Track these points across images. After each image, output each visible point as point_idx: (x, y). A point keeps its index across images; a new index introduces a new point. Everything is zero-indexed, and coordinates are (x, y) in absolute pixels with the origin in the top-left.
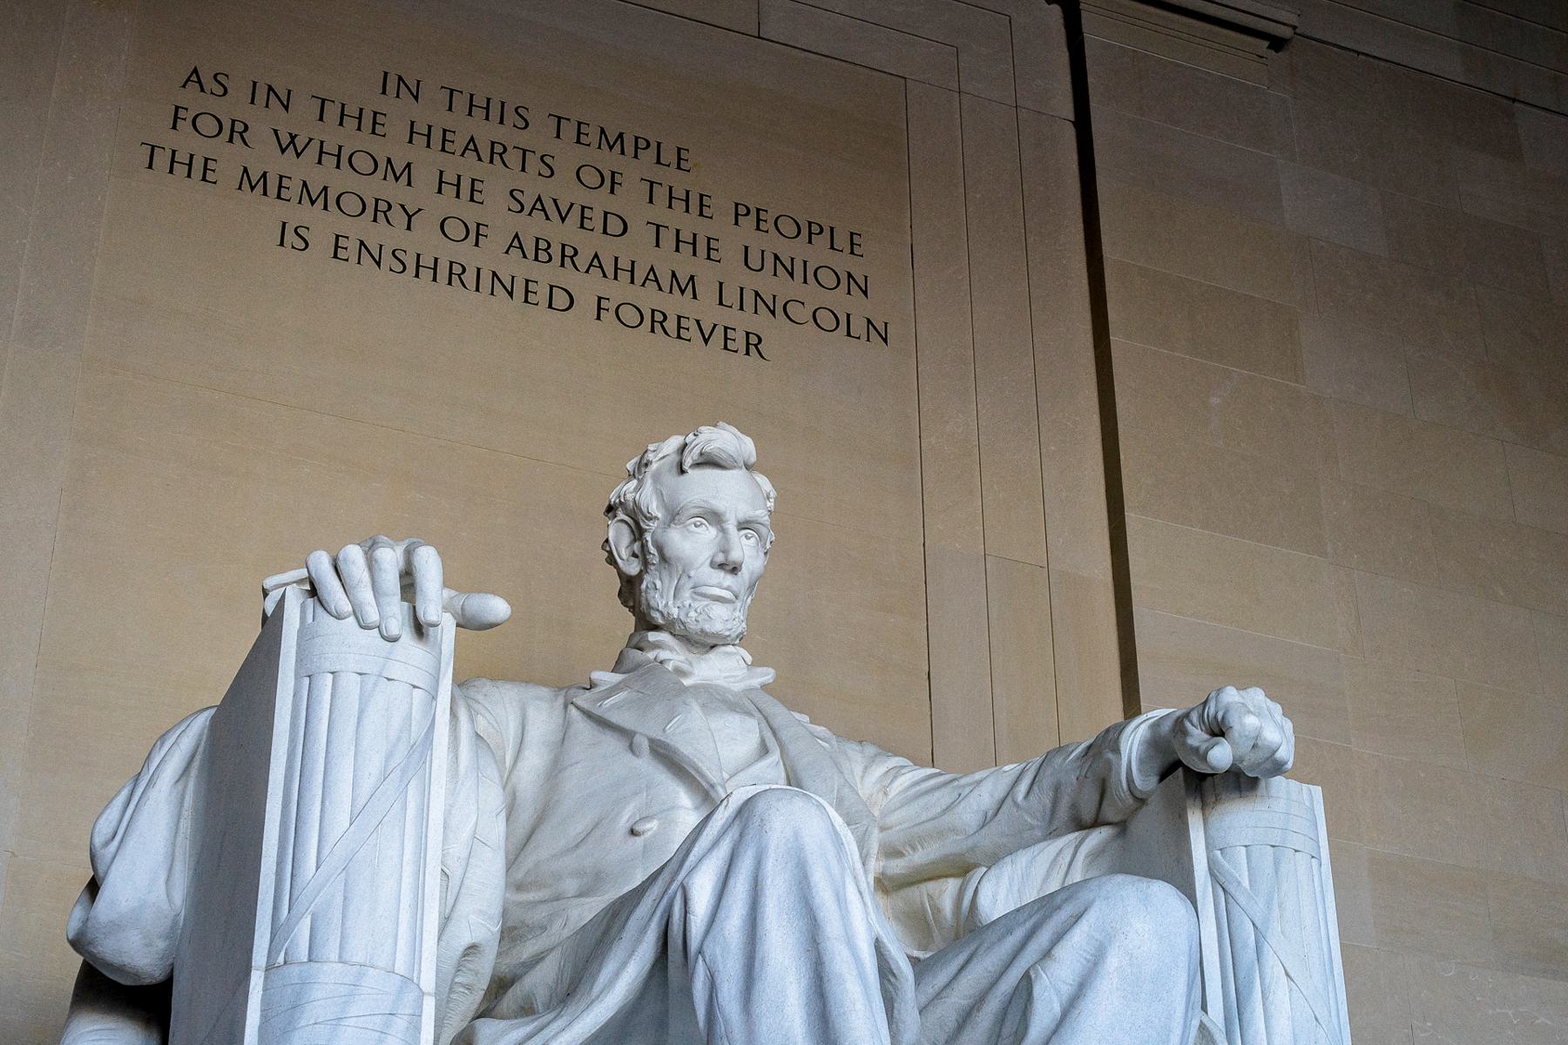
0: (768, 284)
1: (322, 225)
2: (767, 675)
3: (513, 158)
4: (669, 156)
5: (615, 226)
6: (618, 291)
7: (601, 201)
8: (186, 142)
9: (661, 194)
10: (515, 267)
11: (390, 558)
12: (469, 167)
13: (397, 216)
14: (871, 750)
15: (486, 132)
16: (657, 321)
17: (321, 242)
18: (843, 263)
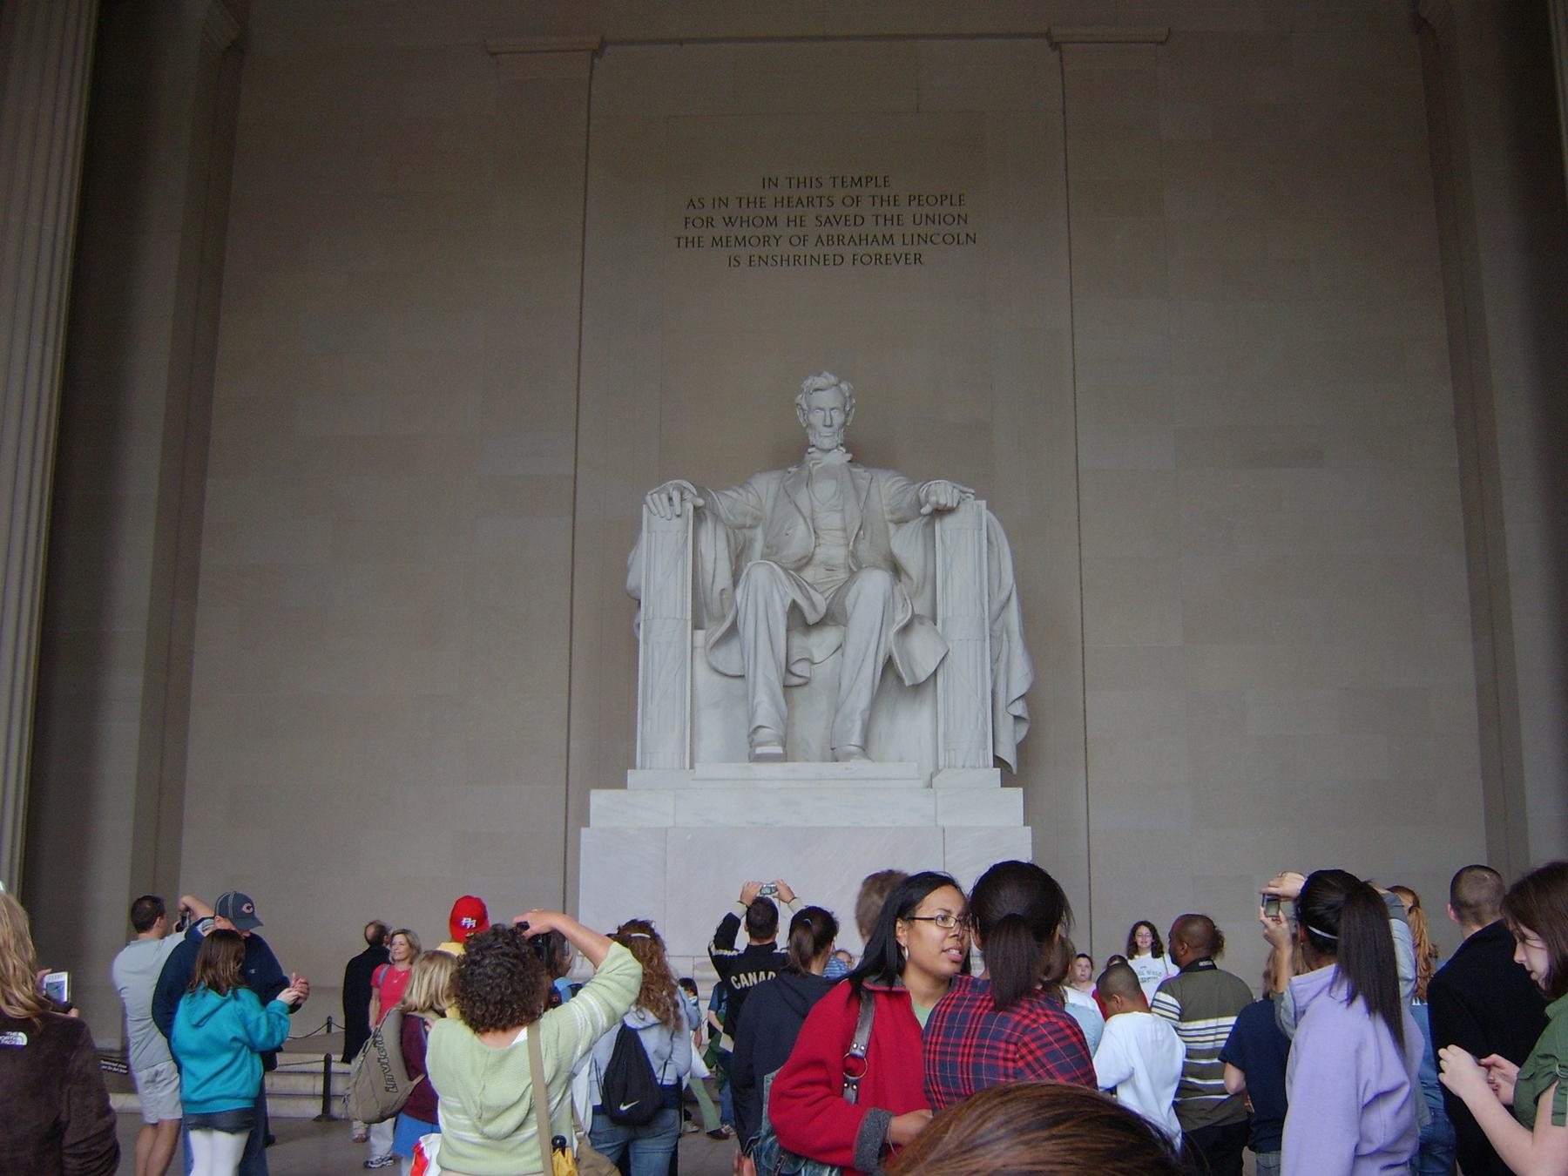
0: (925, 229)
1: (743, 252)
2: (849, 456)
3: (817, 202)
4: (881, 182)
5: (859, 220)
6: (860, 250)
7: (853, 211)
8: (691, 232)
9: (878, 201)
10: (819, 251)
11: (664, 497)
12: (799, 211)
13: (773, 241)
14: (890, 473)
15: (804, 193)
16: (878, 258)
17: (744, 261)
18: (955, 210)
